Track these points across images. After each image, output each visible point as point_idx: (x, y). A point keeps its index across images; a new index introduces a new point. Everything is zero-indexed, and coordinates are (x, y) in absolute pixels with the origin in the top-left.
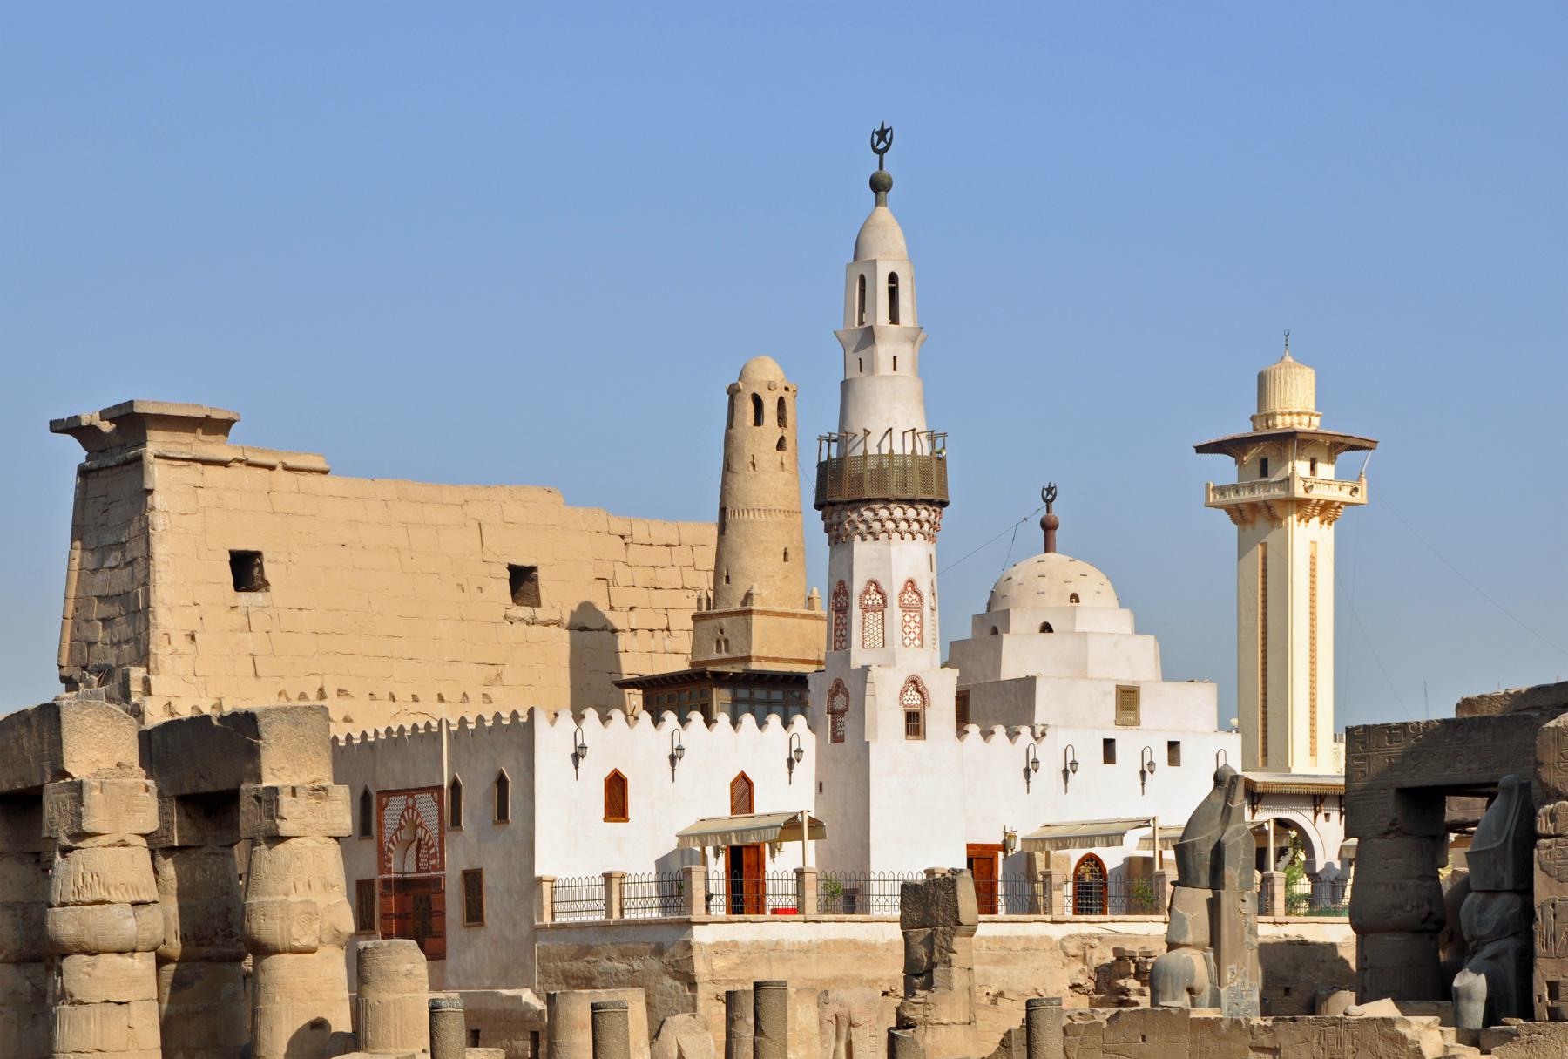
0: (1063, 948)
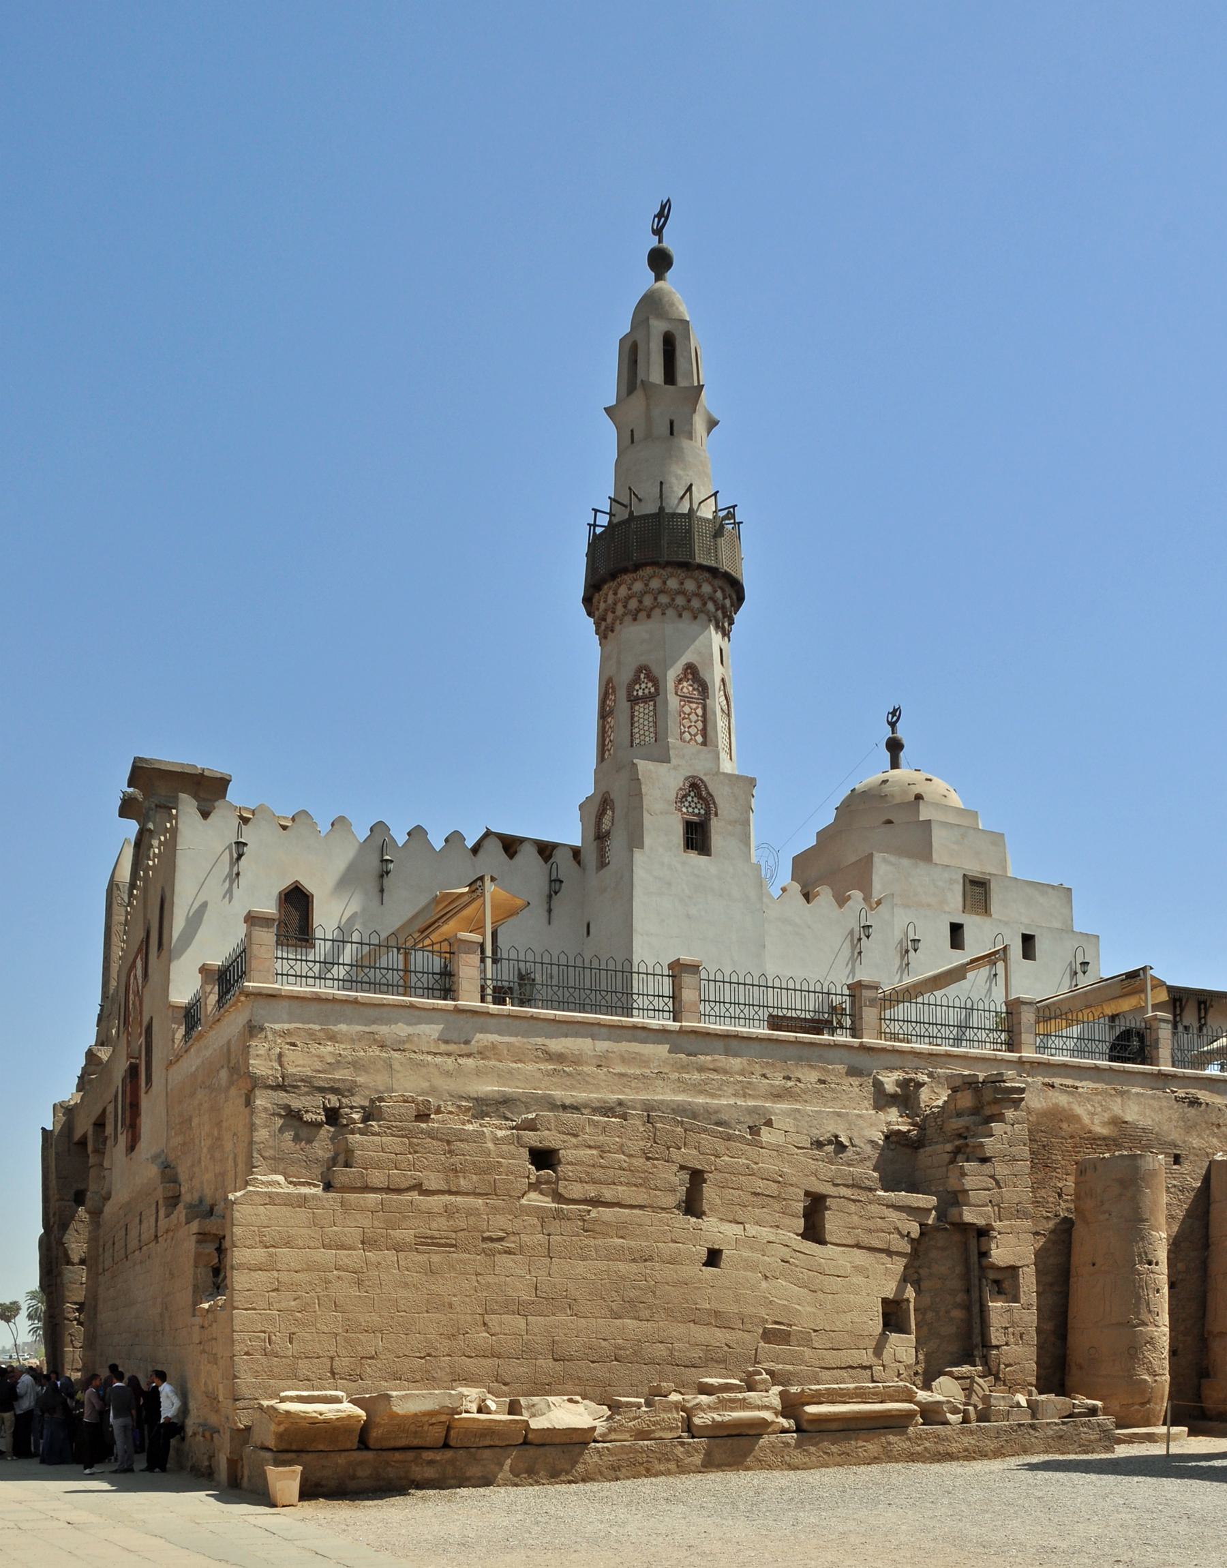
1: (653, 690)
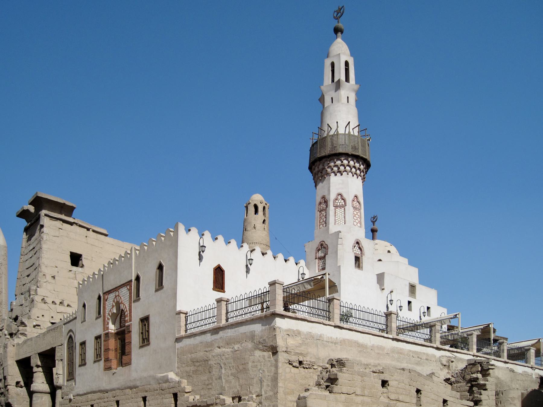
0: (440, 361)
1: (343, 203)
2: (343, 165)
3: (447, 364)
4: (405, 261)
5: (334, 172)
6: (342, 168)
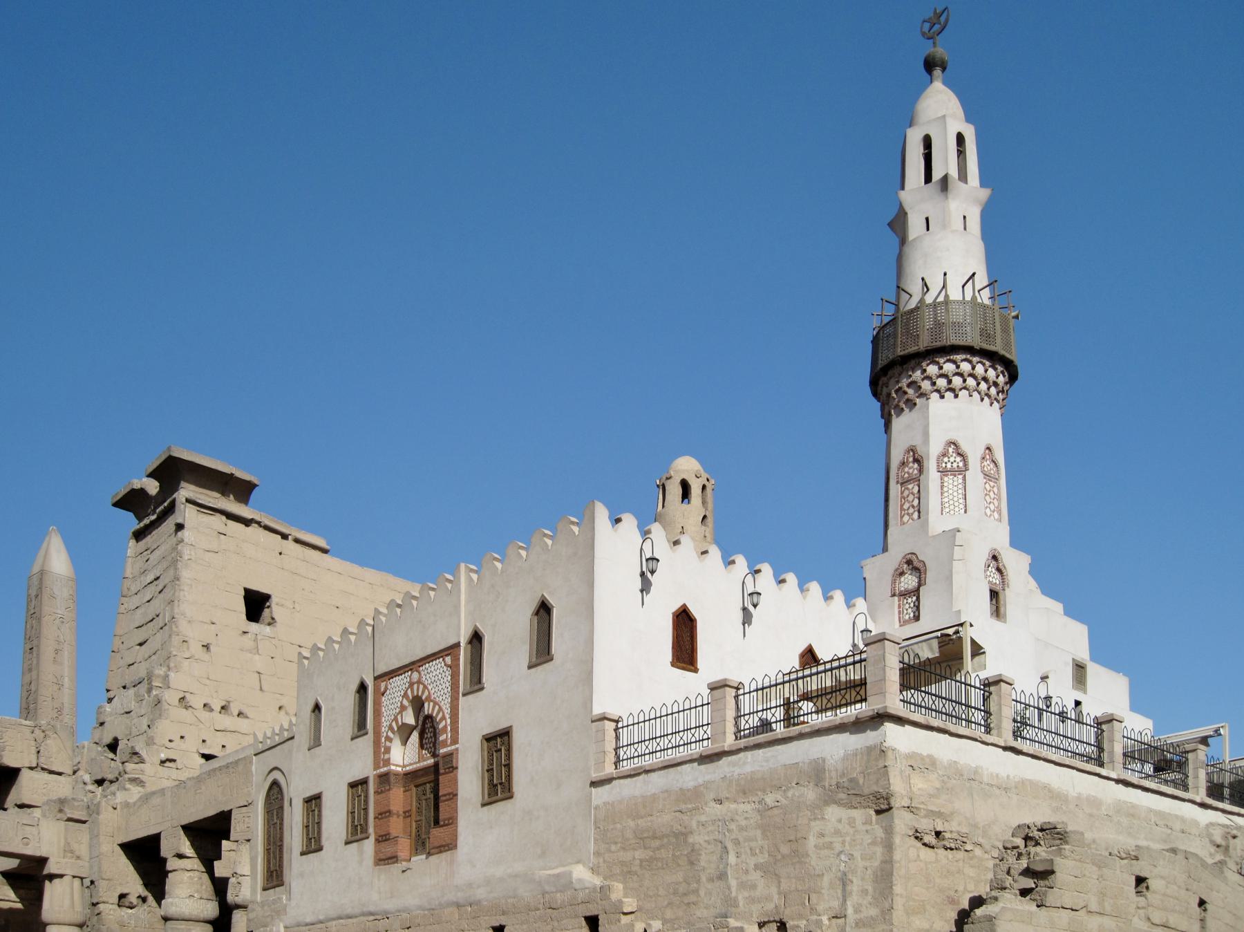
0: (1209, 836)
1: (961, 464)
2: (960, 375)
3: (1223, 843)
4: (1058, 607)
5: (938, 391)
6: (957, 381)
